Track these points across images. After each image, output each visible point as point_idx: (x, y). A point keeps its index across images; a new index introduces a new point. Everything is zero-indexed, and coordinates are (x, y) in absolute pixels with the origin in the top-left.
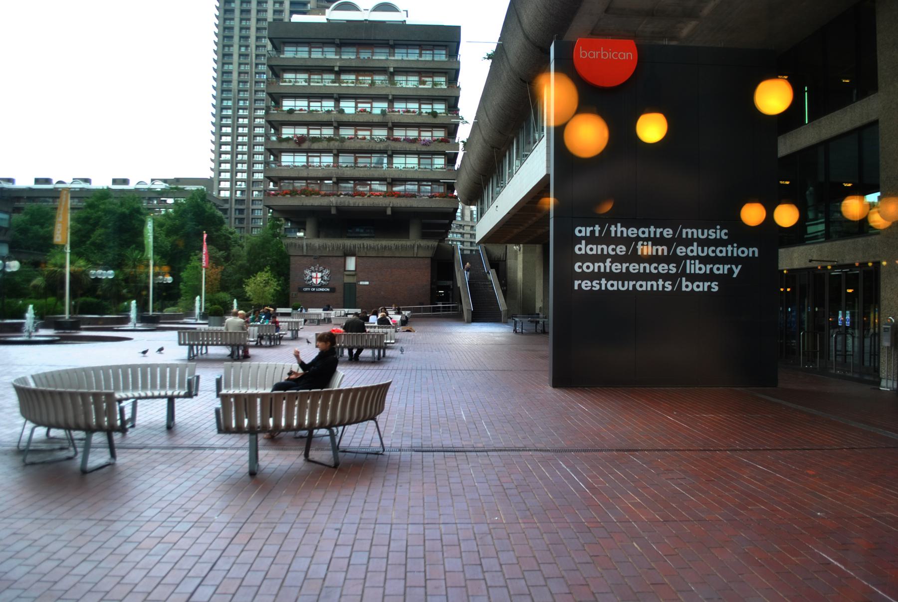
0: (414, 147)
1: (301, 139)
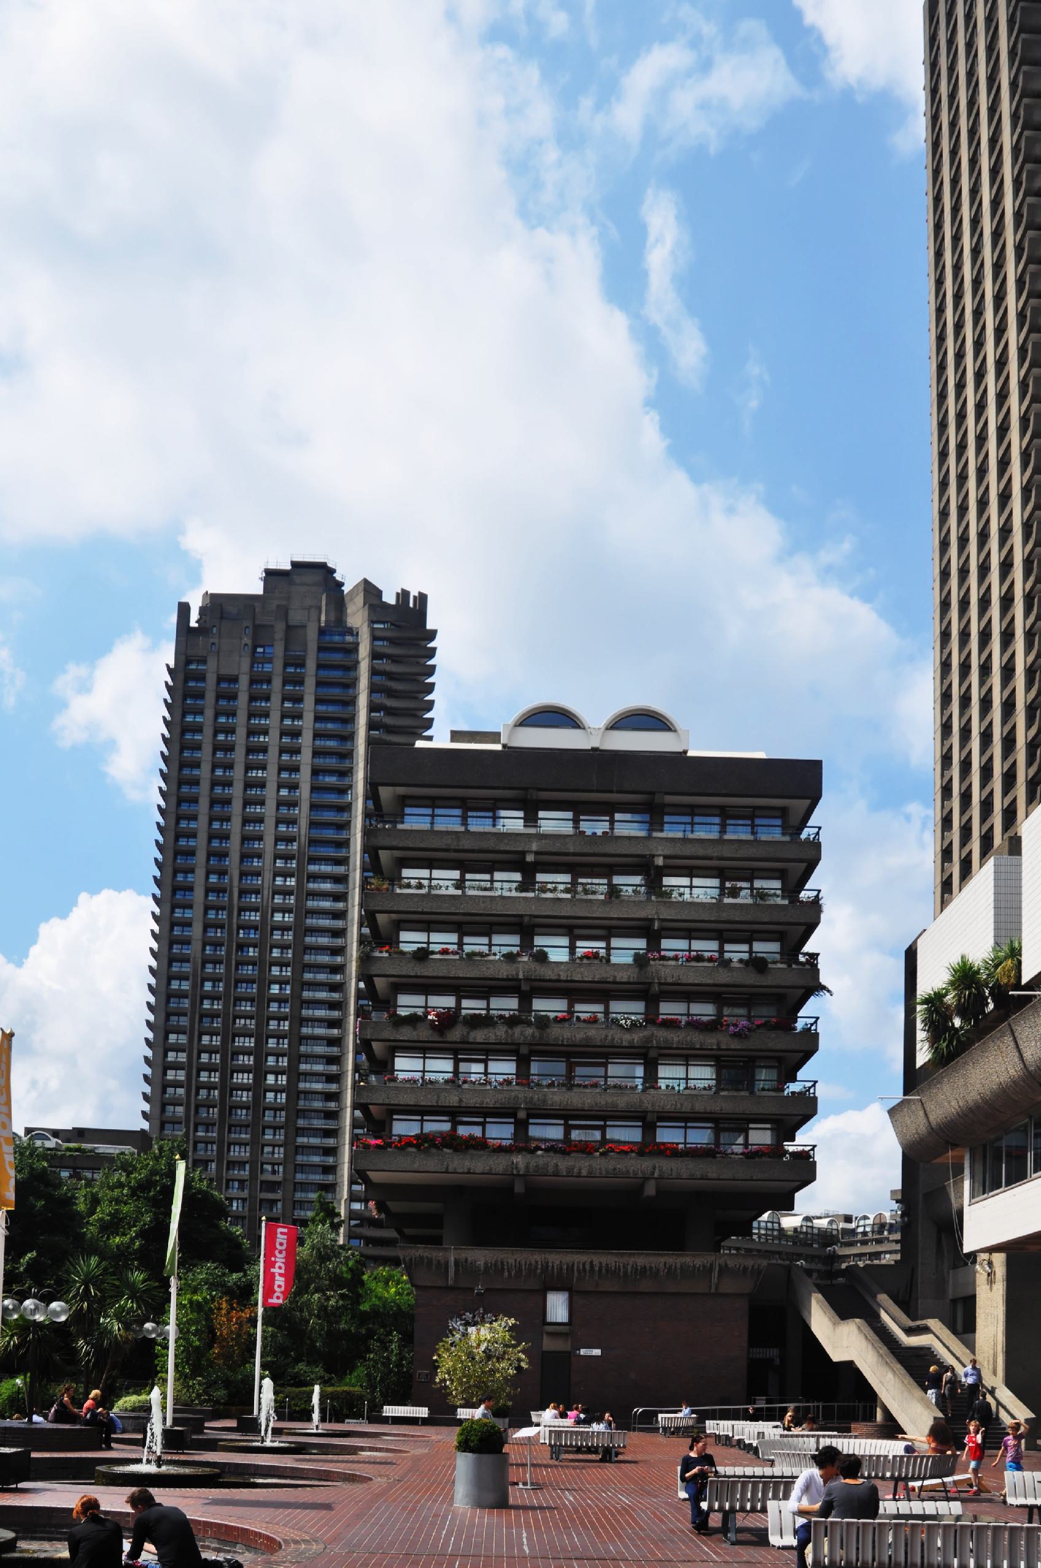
0: (711, 1040)
1: (449, 1019)
